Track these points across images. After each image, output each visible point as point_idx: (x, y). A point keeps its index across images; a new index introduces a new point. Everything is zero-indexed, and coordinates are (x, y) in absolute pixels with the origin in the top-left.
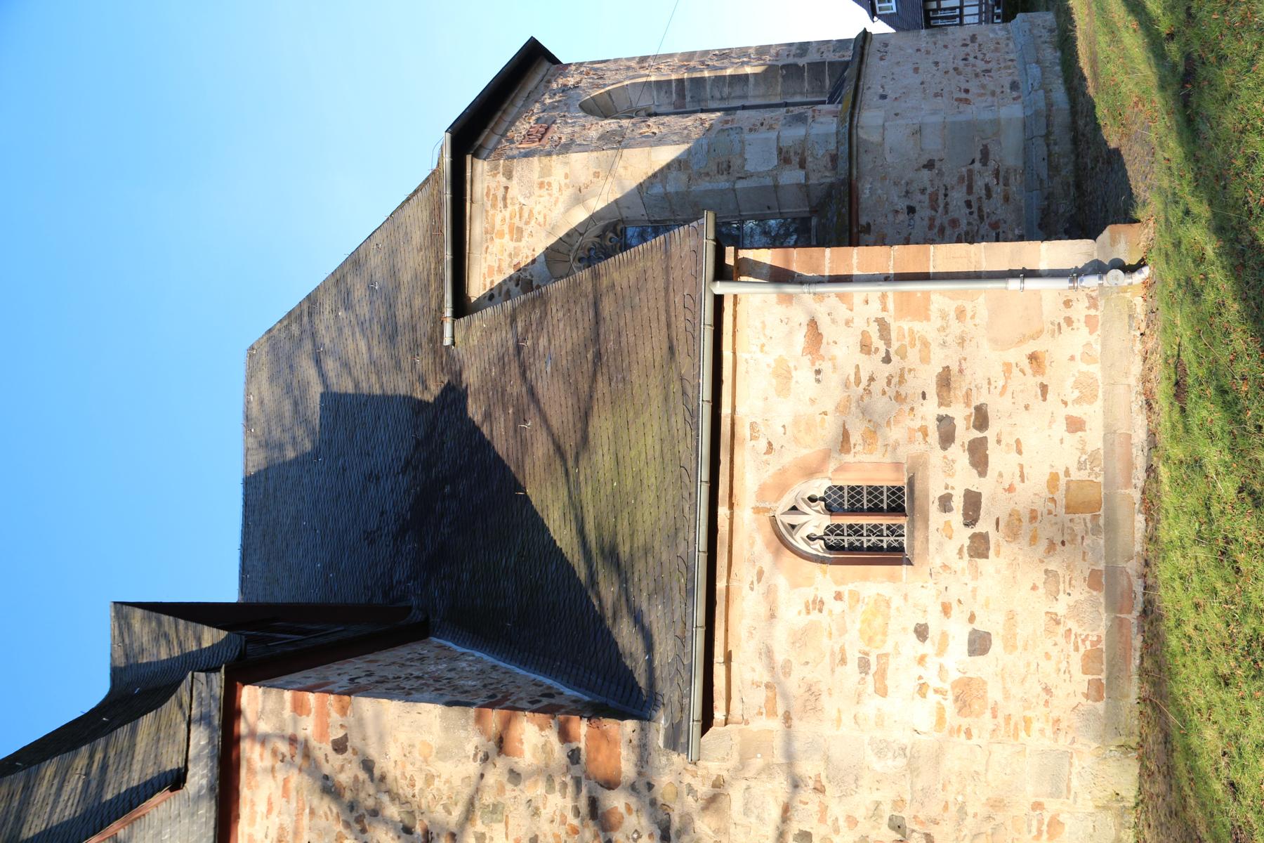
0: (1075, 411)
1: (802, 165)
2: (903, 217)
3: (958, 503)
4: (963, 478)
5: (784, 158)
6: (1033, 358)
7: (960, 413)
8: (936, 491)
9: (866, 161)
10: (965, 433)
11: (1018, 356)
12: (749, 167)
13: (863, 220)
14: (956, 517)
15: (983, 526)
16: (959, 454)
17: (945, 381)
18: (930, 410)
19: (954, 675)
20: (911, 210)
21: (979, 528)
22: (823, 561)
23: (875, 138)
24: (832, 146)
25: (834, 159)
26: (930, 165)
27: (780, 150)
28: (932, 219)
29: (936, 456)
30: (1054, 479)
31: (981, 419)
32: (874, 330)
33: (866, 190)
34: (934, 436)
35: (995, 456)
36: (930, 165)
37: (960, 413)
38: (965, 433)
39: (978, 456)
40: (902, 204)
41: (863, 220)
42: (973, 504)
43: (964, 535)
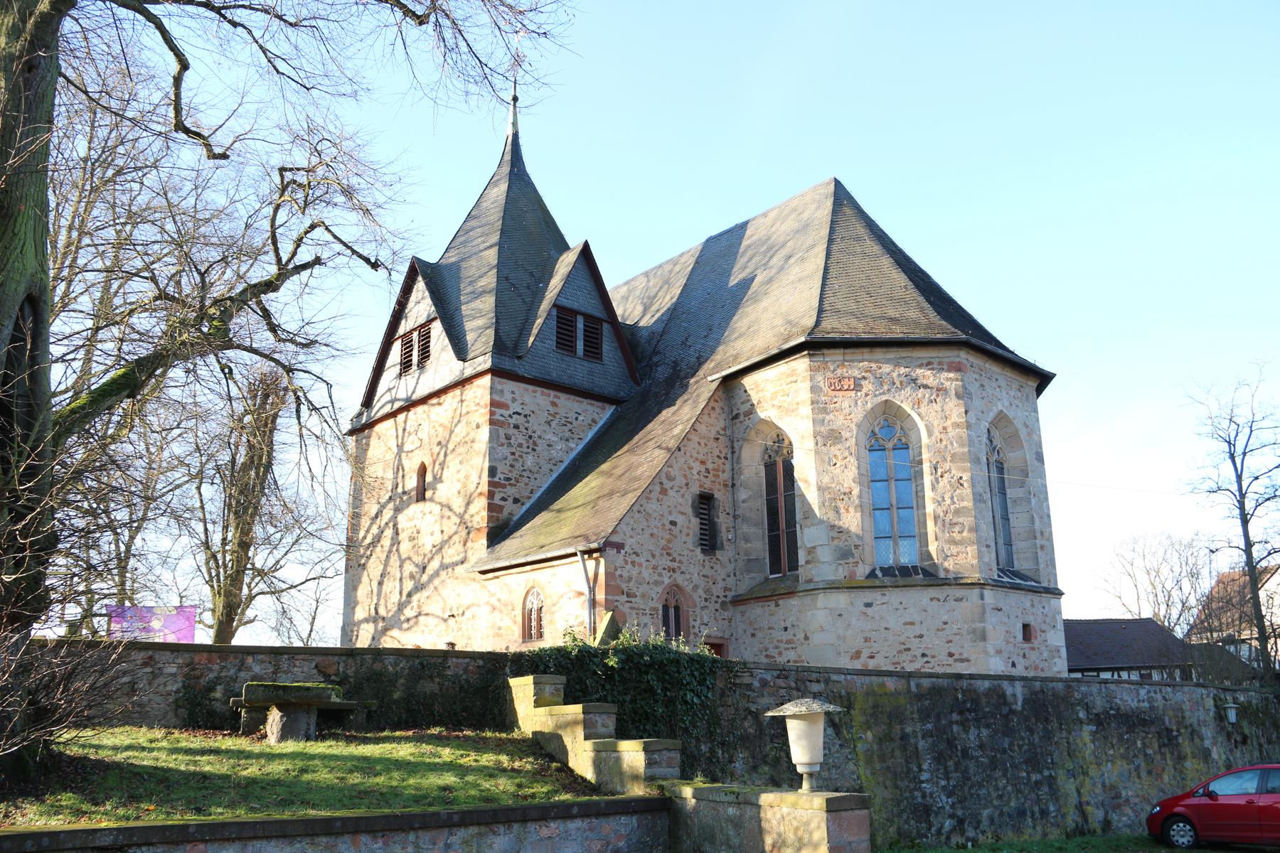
1: (807, 562)
2: (783, 625)
5: (811, 551)
9: (808, 600)
12: (806, 531)
13: (781, 602)
20: (786, 629)
22: (524, 608)
23: (820, 604)
24: (816, 579)
25: (810, 581)
26: (806, 638)
27: (814, 548)
28: (781, 641)
33: (794, 602)
36: (806, 638)
40: (788, 624)
41: (781, 602)
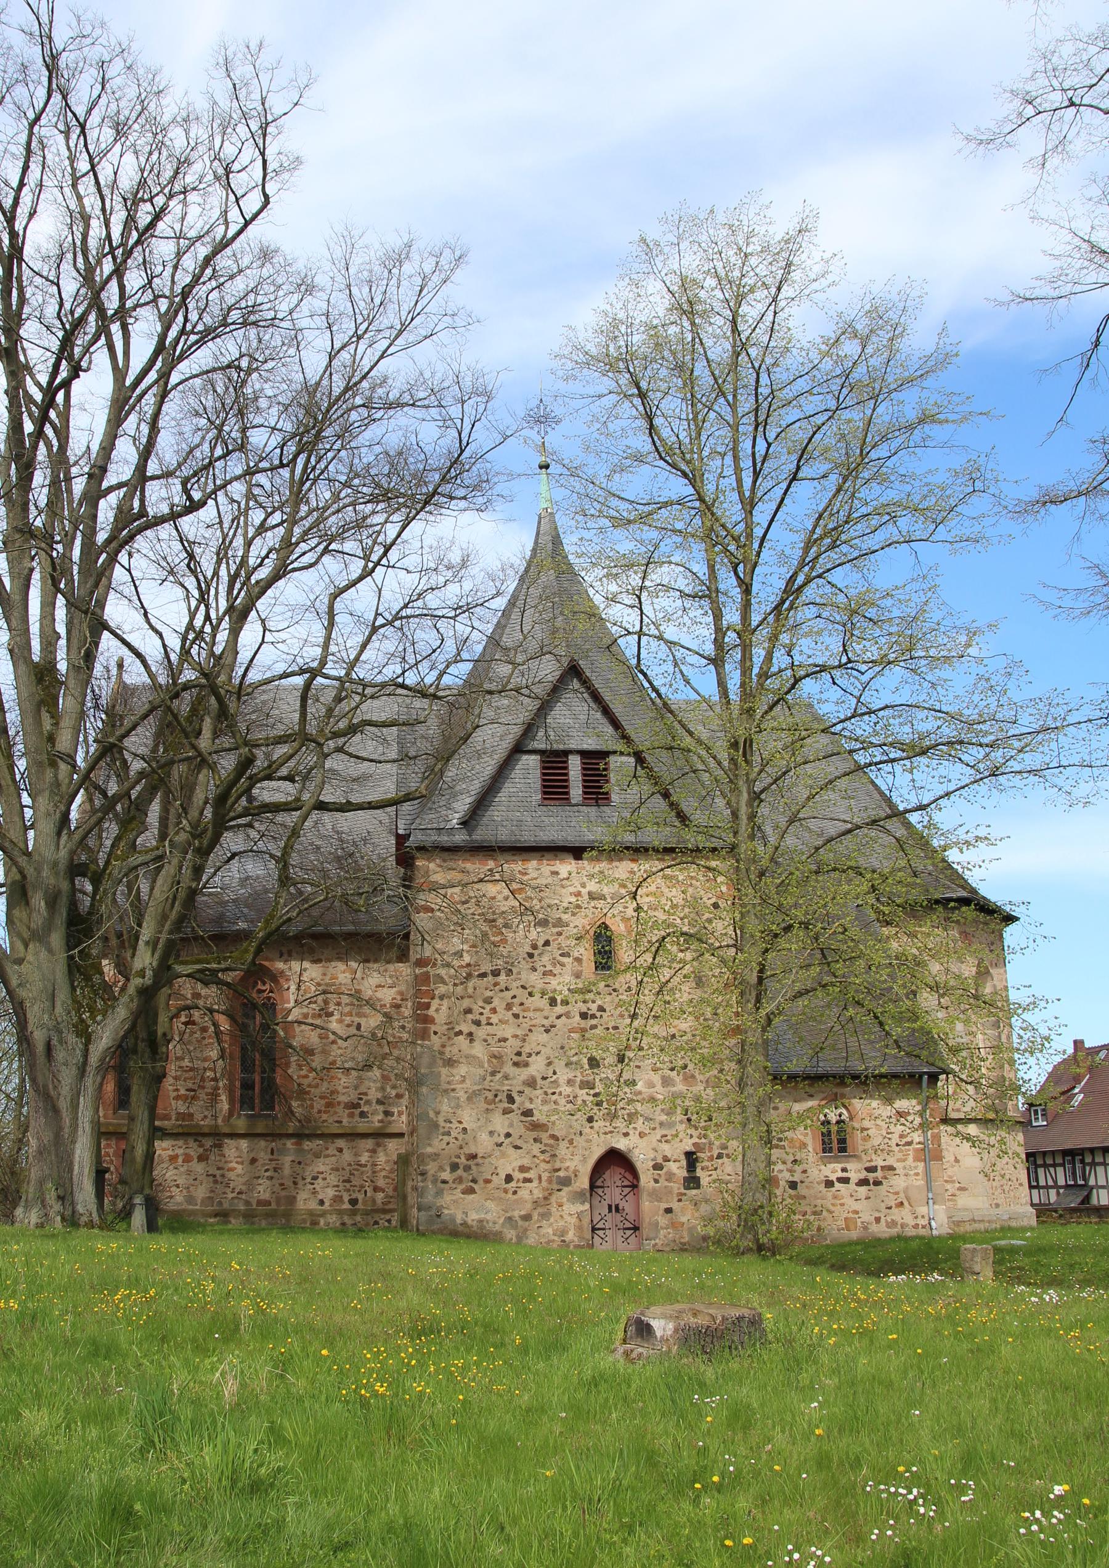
0: (883, 1220)
3: (845, 1175)
4: (854, 1177)
6: (902, 1203)
7: (879, 1174)
8: (849, 1166)
10: (871, 1176)
11: (901, 1197)
14: (840, 1174)
15: (837, 1184)
16: (864, 1174)
17: (891, 1168)
18: (879, 1162)
19: (780, 1176)
21: (837, 1184)
29: (860, 1166)
30: (857, 1212)
31: (877, 1183)
32: (909, 1139)
34: (868, 1165)
35: (863, 1190)
37: (879, 1174)
38: (871, 1176)
39: (863, 1182)
42: (845, 1181)
43: (833, 1177)
